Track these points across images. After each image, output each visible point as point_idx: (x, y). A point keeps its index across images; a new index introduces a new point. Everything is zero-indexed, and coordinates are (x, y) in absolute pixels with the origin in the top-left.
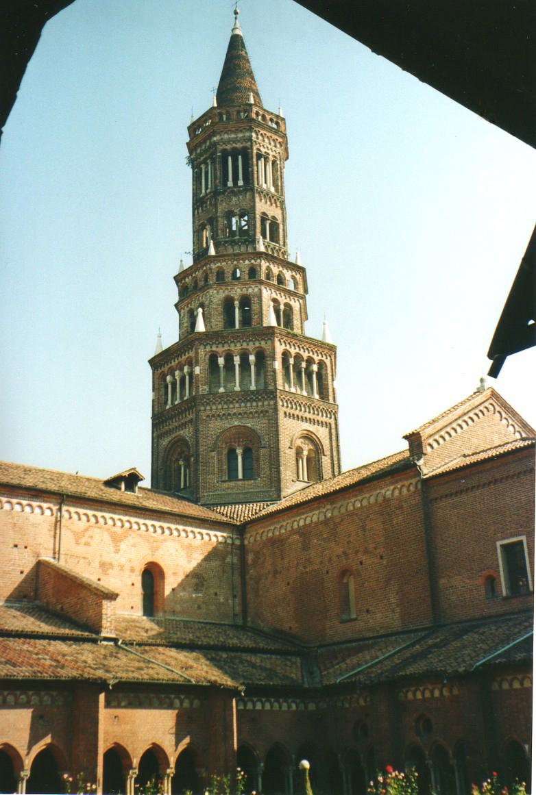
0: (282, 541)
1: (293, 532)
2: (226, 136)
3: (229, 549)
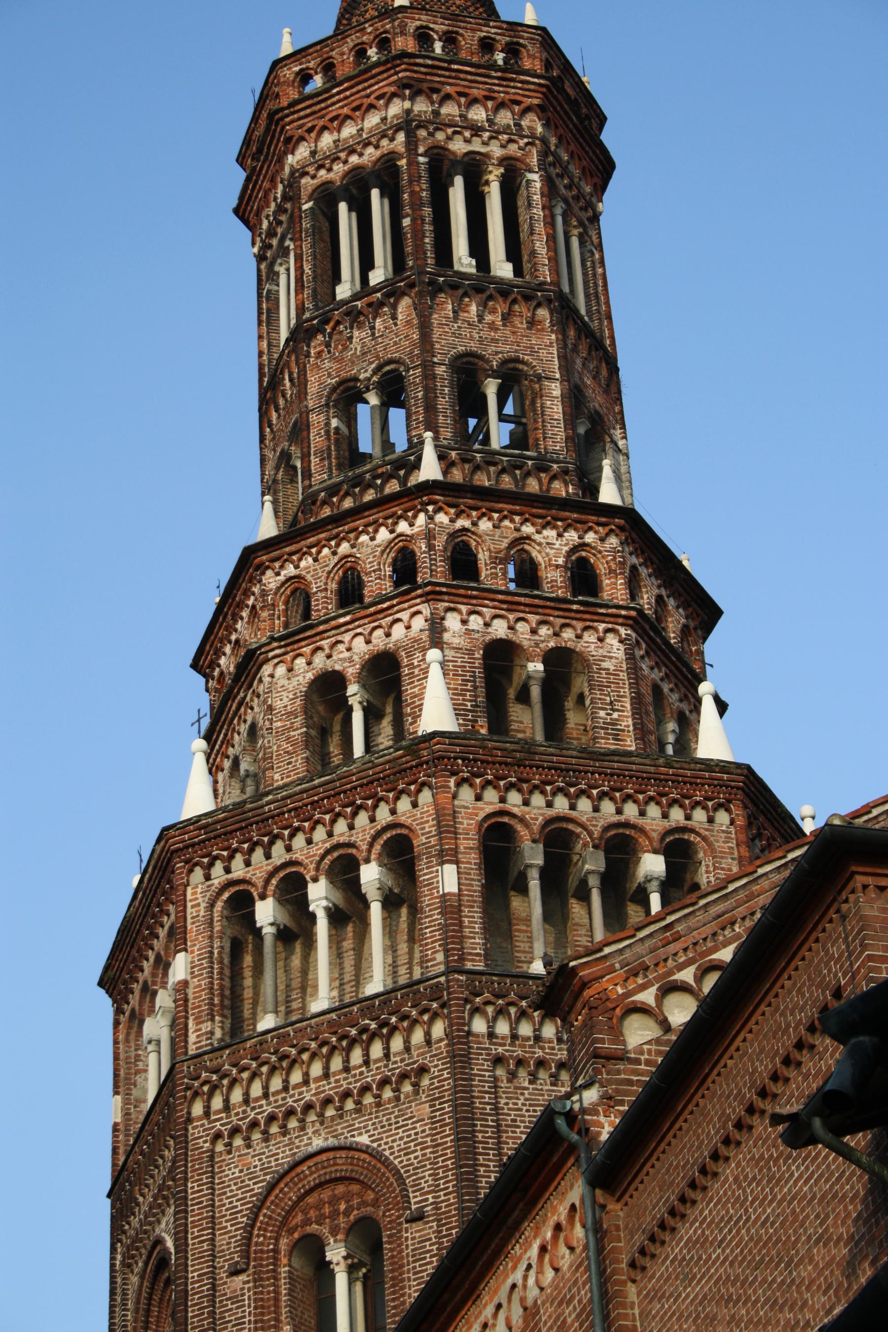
2: (327, 140)
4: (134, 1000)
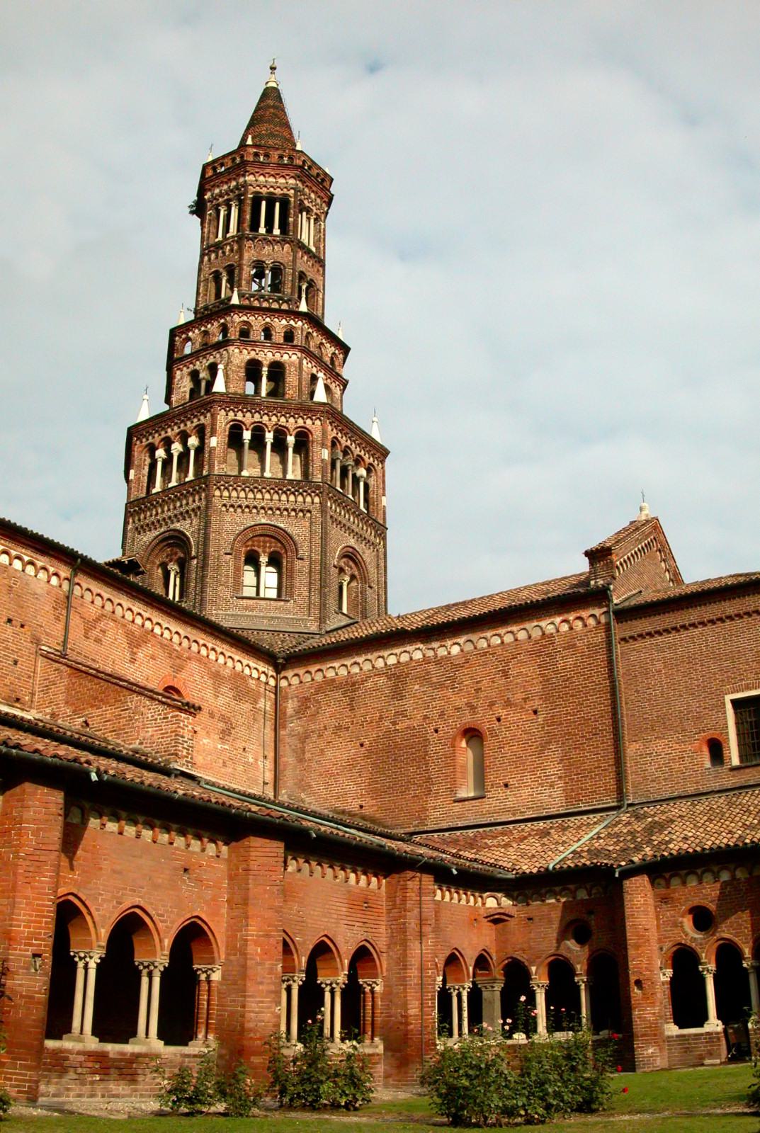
0: (354, 684)
1: (375, 672)
3: (262, 690)
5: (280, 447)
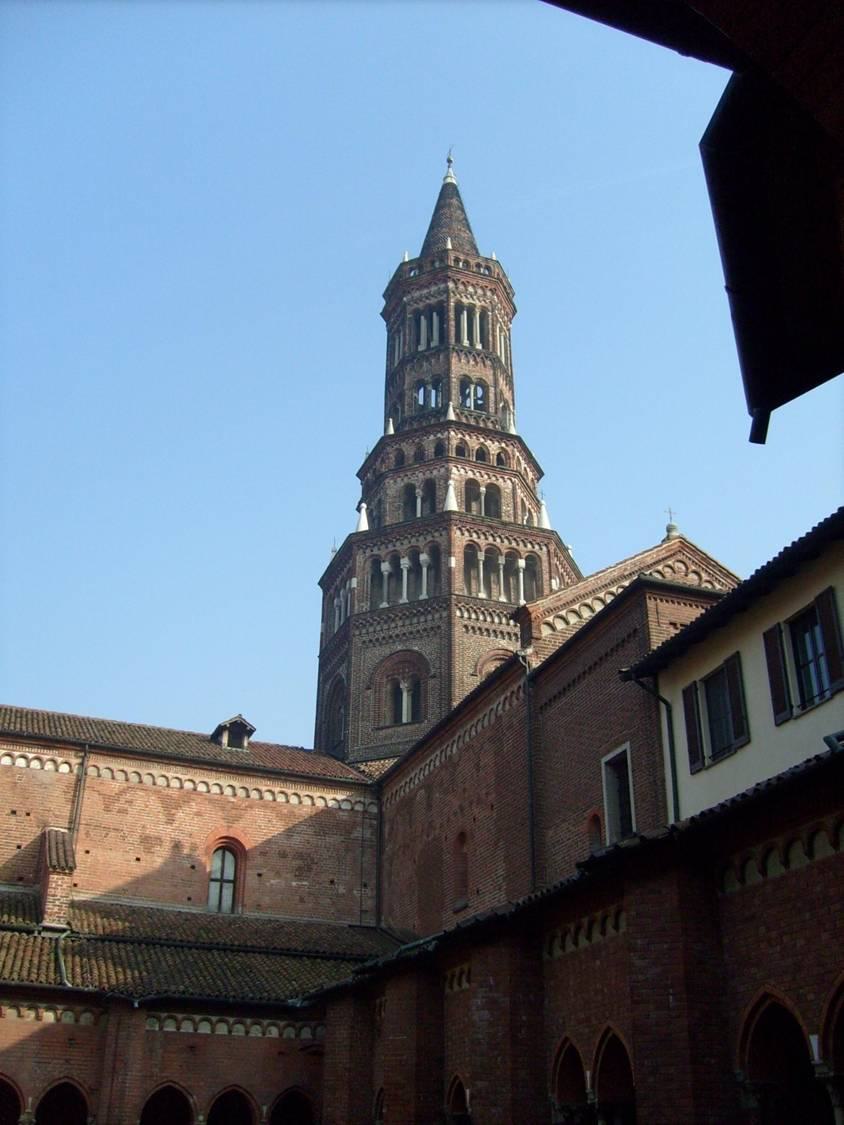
2: (417, 294)
4: (332, 591)
5: (415, 569)
